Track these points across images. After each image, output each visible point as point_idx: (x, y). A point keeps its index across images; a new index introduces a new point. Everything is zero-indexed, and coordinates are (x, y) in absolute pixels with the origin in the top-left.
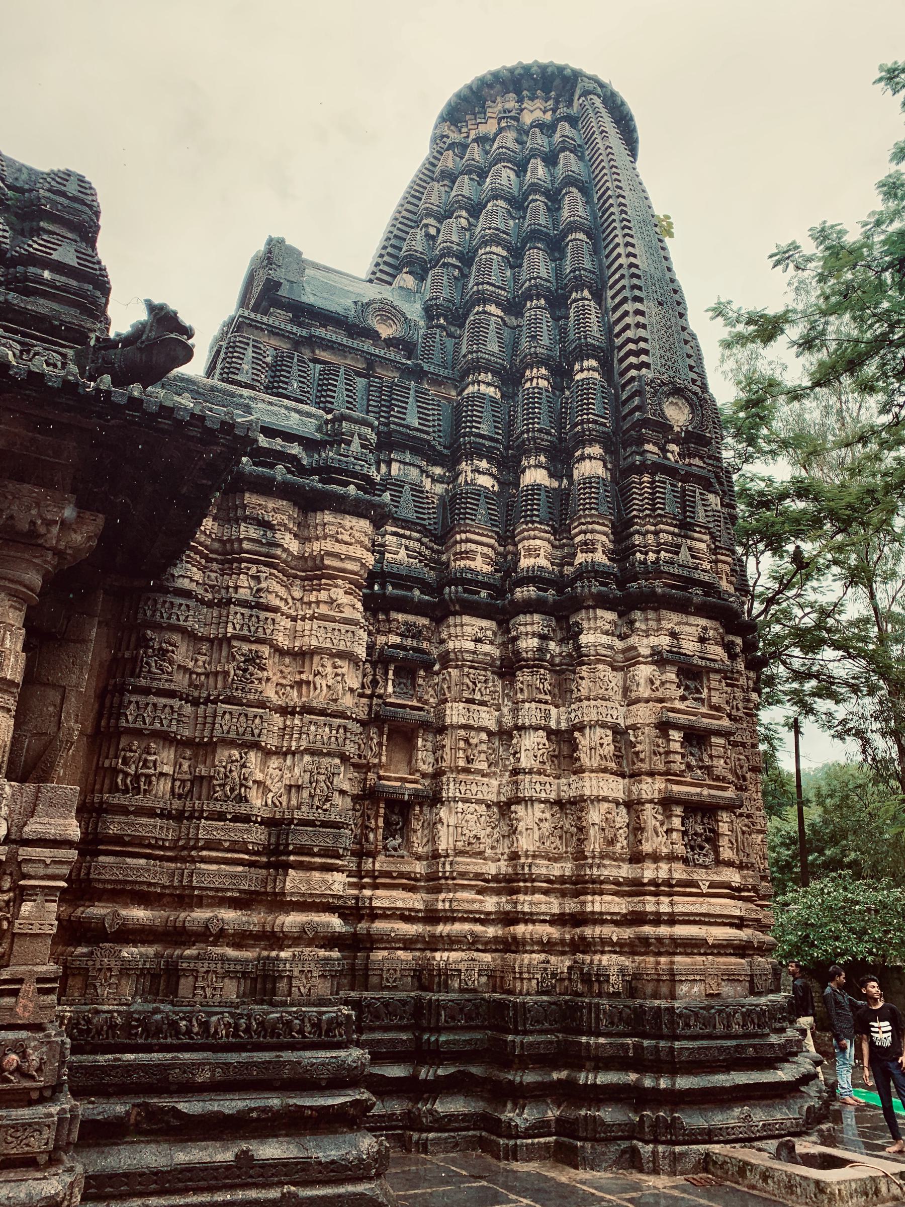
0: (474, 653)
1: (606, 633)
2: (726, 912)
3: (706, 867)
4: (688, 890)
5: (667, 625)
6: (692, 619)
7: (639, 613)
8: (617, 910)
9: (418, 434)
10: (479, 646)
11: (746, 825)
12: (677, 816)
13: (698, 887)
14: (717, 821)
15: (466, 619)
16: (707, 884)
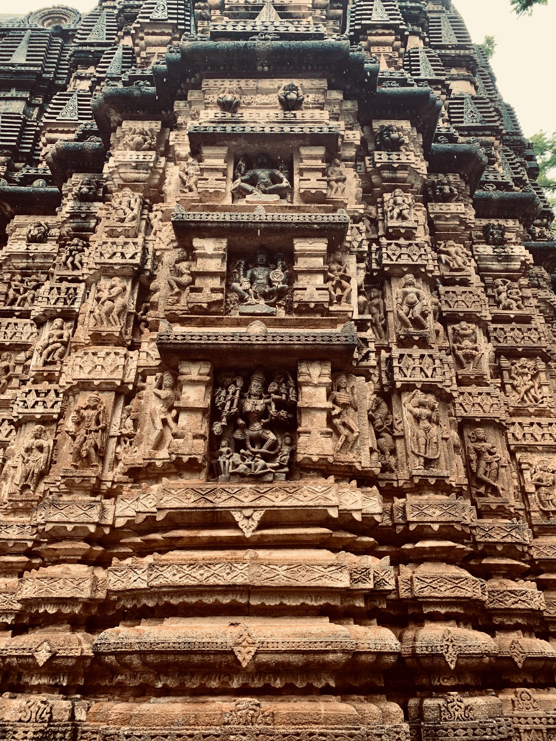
0: (26, 256)
1: (138, 147)
2: (303, 582)
3: (257, 479)
4: (205, 533)
5: (214, 98)
6: (265, 84)
7: (182, 104)
8: (66, 593)
9: (27, 68)
10: (33, 247)
11: (421, 405)
12: (194, 383)
13: (235, 525)
14: (298, 386)
15: (18, 219)
16: (258, 516)
